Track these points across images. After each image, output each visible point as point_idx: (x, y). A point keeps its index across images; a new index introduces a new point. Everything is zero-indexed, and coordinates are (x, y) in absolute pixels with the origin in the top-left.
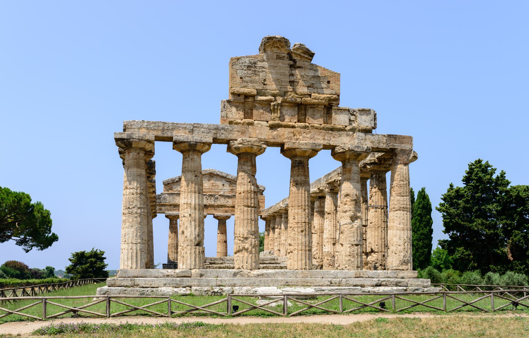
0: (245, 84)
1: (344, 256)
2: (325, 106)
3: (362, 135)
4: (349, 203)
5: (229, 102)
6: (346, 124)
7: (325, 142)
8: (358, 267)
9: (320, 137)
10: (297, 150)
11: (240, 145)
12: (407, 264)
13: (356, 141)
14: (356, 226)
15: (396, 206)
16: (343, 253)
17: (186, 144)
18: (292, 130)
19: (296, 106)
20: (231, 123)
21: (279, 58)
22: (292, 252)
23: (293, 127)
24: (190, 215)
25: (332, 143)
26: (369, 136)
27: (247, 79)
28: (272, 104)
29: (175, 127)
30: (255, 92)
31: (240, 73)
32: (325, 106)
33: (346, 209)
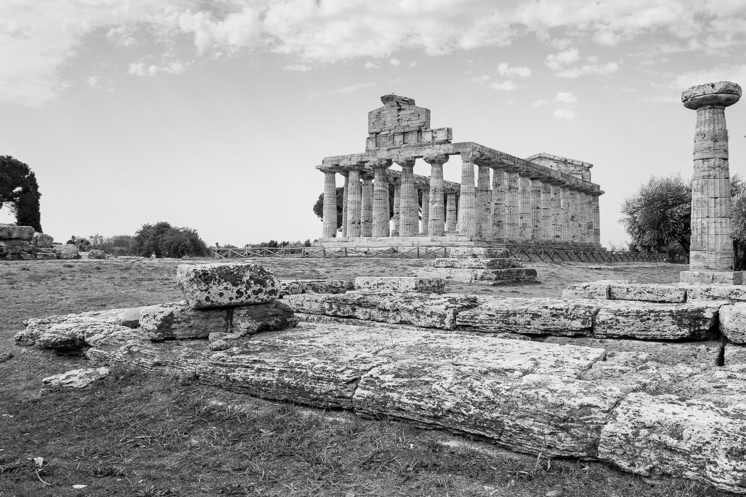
2: (418, 131)
5: (368, 138)
6: (431, 140)
7: (416, 155)
8: (434, 234)
9: (414, 152)
12: (465, 231)
13: (435, 151)
14: (433, 208)
18: (399, 150)
20: (368, 151)
21: (392, 106)
23: (399, 148)
25: (420, 155)
26: (443, 145)
29: (344, 157)
31: (373, 121)
32: (418, 131)
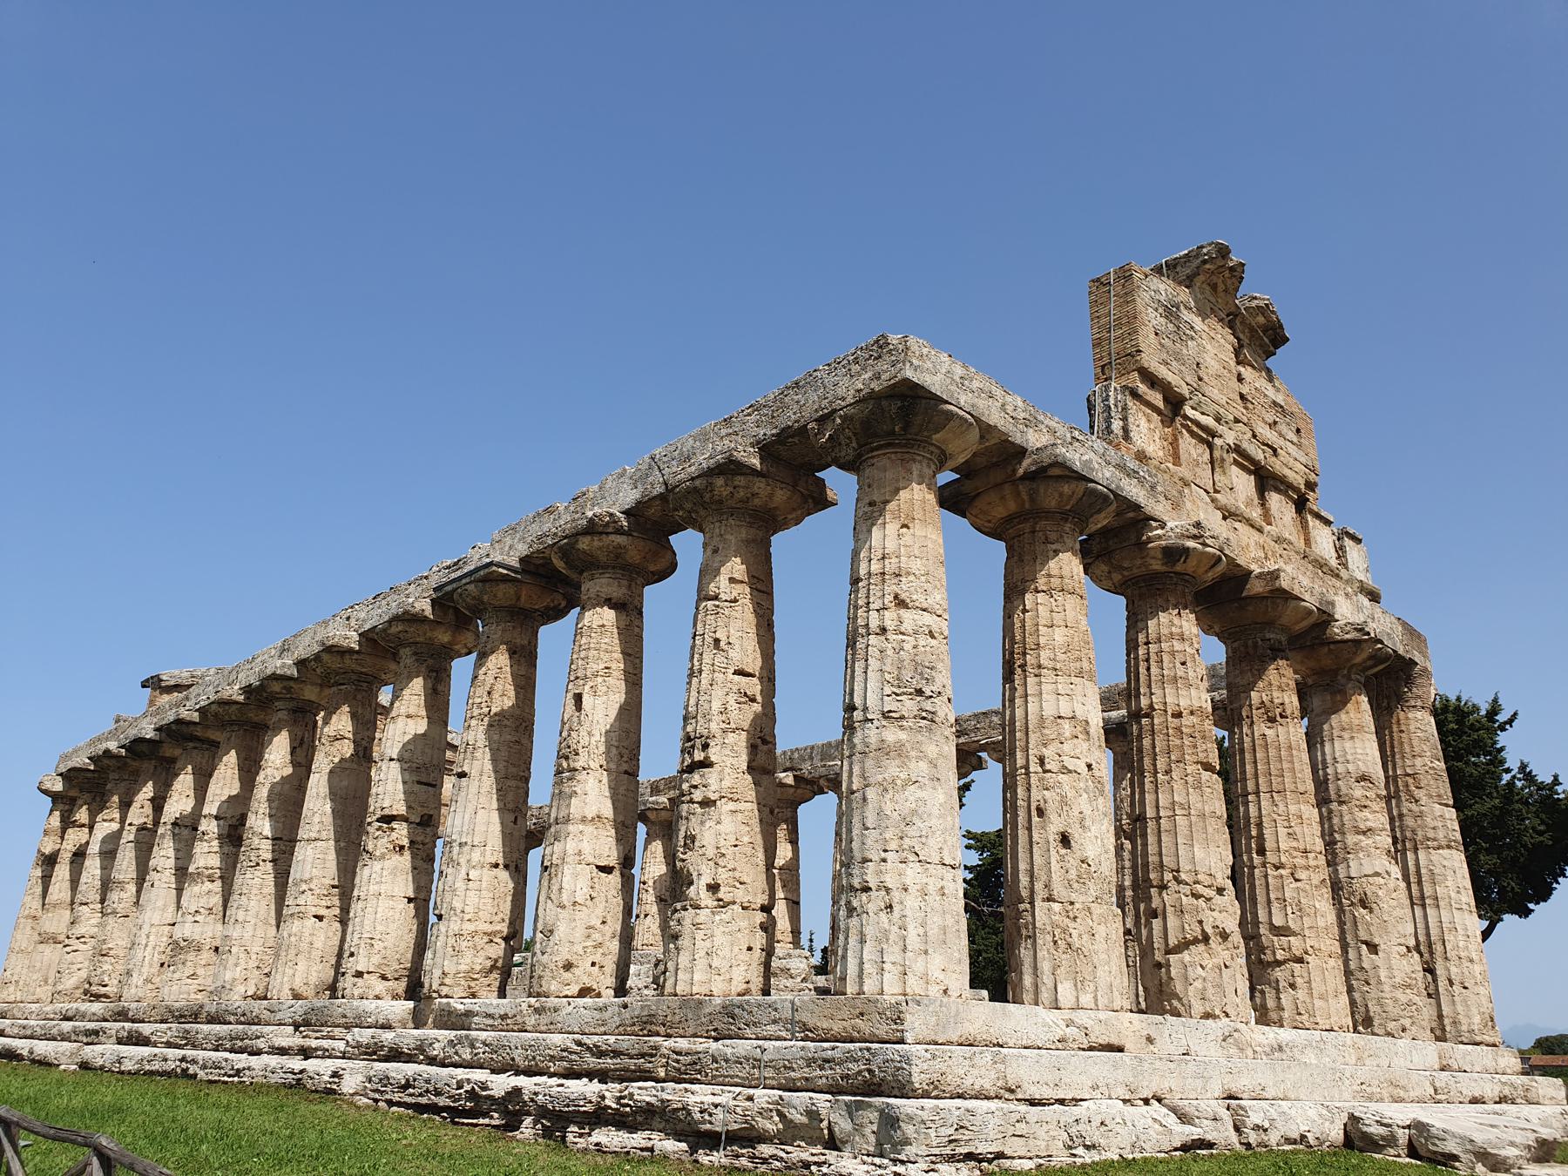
0: (1165, 356)
1: (1387, 988)
3: (1366, 602)
4: (1375, 806)
10: (1293, 603)
11: (1191, 544)
15: (1441, 835)
16: (1383, 974)
17: (1082, 486)
19: (1249, 472)
22: (1300, 960)
23: (1260, 530)
24: (1089, 766)
27: (1166, 342)
28: (1218, 442)
30: (1185, 391)
33: (1369, 824)
